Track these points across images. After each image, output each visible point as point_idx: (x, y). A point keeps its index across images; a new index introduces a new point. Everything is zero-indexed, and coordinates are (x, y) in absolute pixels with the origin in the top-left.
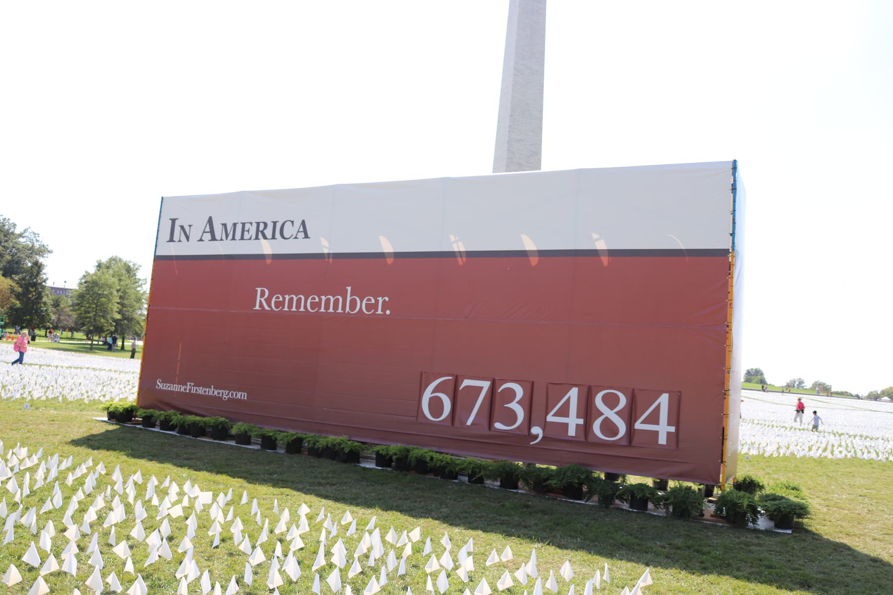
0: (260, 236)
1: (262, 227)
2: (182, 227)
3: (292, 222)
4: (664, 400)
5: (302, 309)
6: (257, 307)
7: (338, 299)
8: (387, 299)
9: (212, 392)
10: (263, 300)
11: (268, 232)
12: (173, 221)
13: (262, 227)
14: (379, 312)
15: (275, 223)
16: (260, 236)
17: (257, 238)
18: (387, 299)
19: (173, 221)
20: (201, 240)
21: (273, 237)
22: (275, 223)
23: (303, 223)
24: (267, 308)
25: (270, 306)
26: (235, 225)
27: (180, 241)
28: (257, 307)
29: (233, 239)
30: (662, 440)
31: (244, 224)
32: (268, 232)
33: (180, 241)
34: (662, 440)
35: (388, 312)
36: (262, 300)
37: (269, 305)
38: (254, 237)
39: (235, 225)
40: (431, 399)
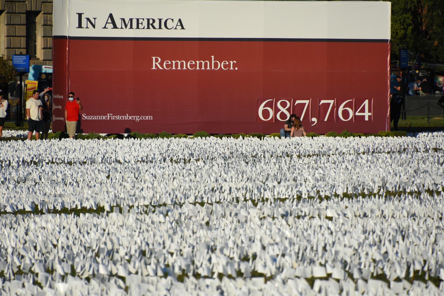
0: (151, 27)
1: (151, 22)
2: (88, 19)
3: (173, 20)
4: (366, 102)
5: (185, 68)
6: (154, 68)
7: (207, 62)
8: (235, 62)
9: (127, 117)
10: (157, 64)
11: (156, 25)
12: (80, 15)
13: (151, 22)
14: (232, 68)
15: (160, 20)
16: (151, 27)
17: (148, 28)
18: (235, 62)
19: (80, 15)
20: (105, 28)
21: (160, 28)
22: (160, 20)
23: (180, 20)
24: (161, 68)
25: (162, 66)
26: (131, 20)
27: (87, 28)
28: (154, 68)
29: (131, 27)
30: (367, 119)
31: (138, 20)
32: (156, 25)
33: (87, 28)
34: (367, 119)
35: (236, 69)
36: (156, 63)
37: (162, 66)
38: (146, 27)
39: (131, 20)
40: (263, 110)
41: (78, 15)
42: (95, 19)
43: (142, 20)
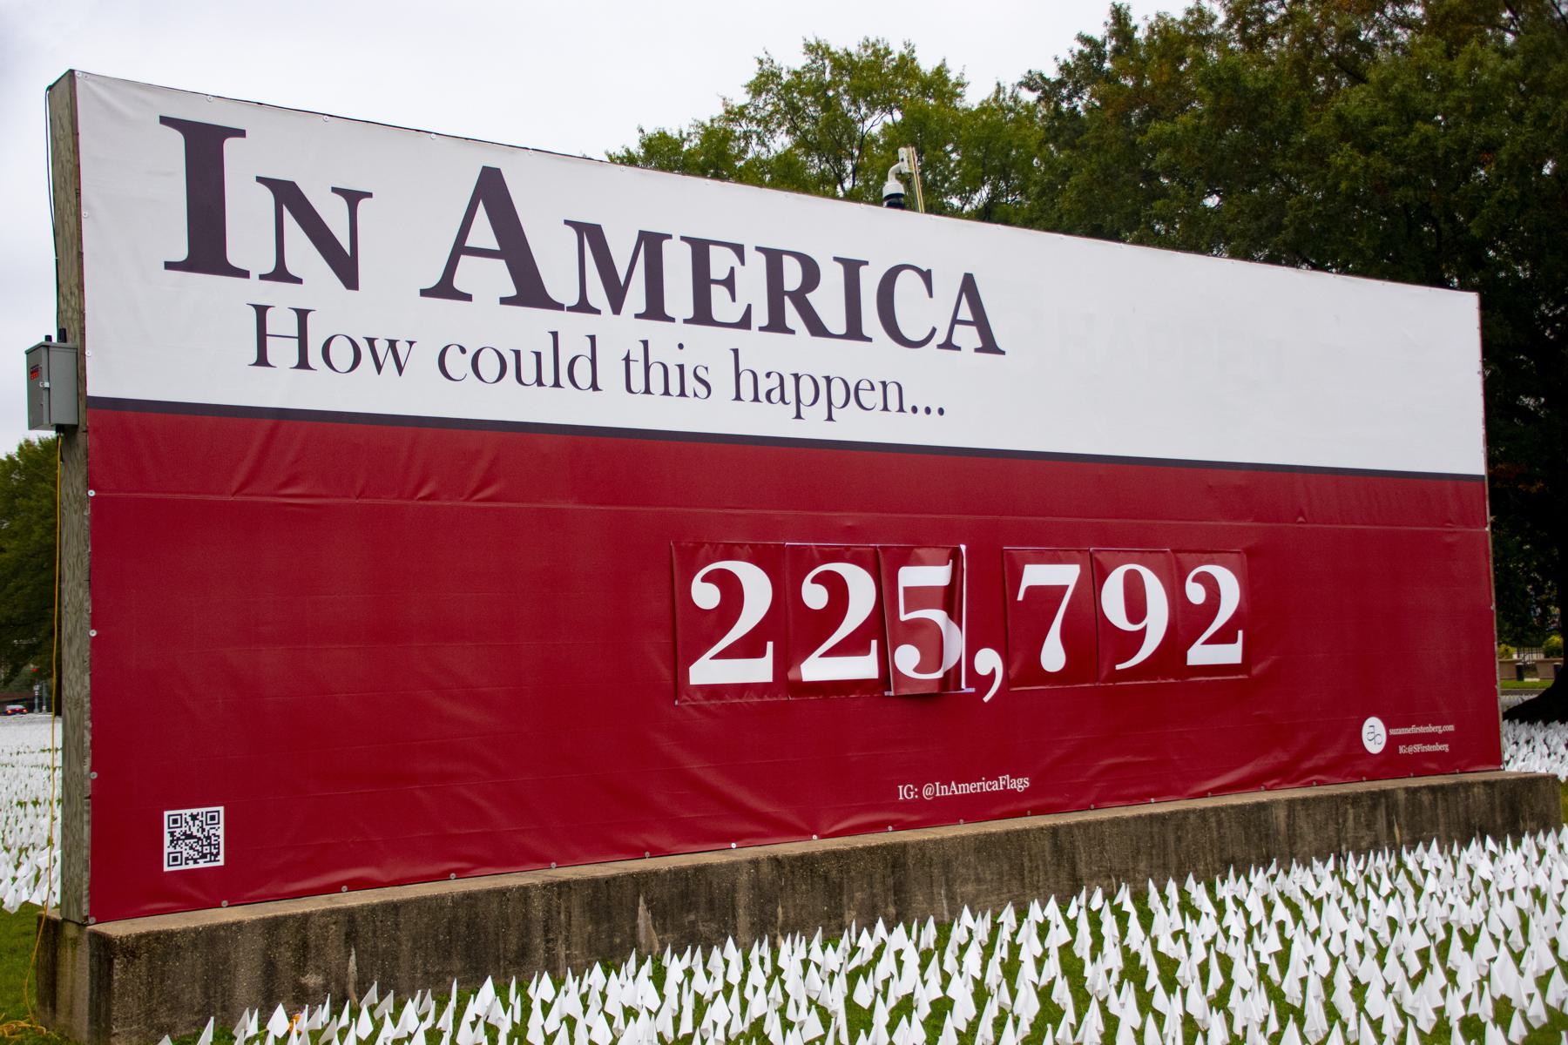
0: (792, 316)
1: (793, 277)
2: (287, 196)
3: (927, 276)
11: (829, 301)
13: (793, 277)
15: (852, 269)
16: (792, 316)
20: (445, 289)
21: (854, 331)
22: (852, 269)
23: (969, 286)
32: (829, 301)
38: (761, 317)
41: (177, 140)
42: (353, 198)
43: (733, 259)
